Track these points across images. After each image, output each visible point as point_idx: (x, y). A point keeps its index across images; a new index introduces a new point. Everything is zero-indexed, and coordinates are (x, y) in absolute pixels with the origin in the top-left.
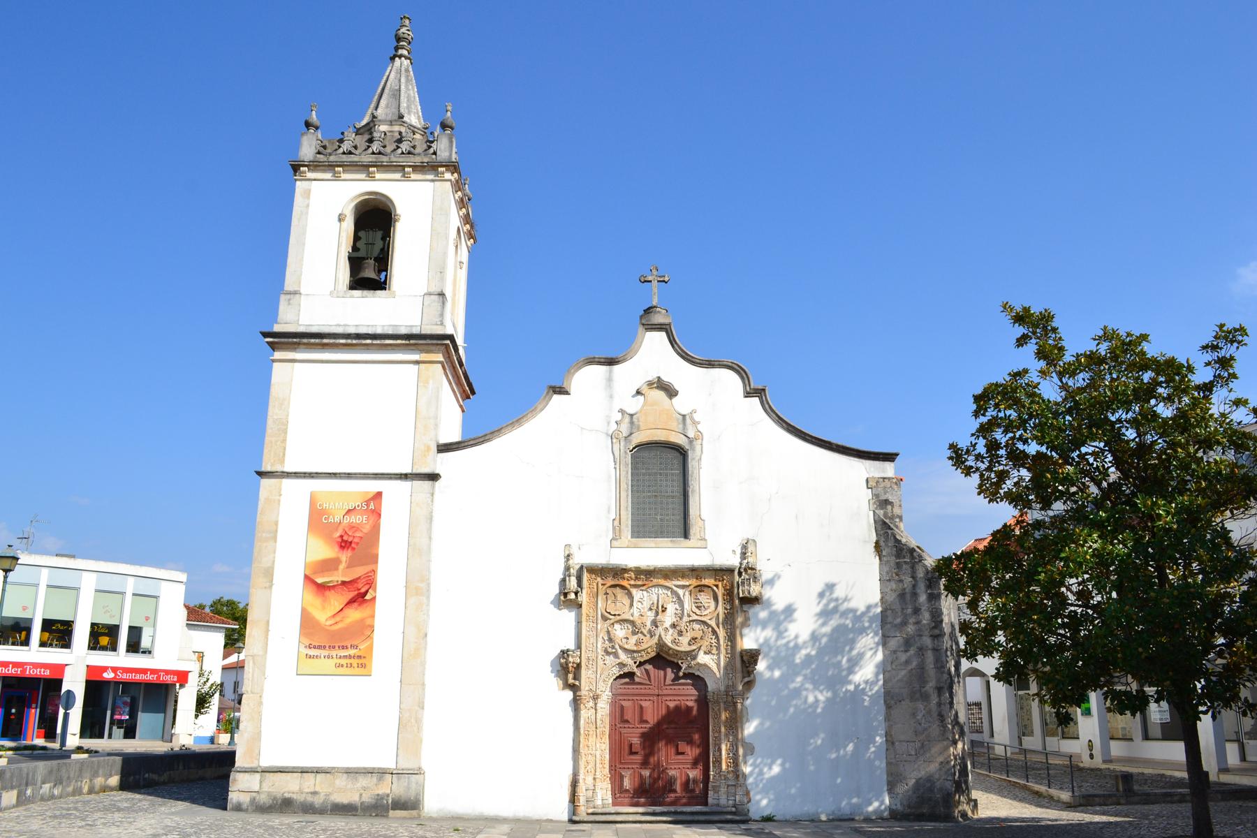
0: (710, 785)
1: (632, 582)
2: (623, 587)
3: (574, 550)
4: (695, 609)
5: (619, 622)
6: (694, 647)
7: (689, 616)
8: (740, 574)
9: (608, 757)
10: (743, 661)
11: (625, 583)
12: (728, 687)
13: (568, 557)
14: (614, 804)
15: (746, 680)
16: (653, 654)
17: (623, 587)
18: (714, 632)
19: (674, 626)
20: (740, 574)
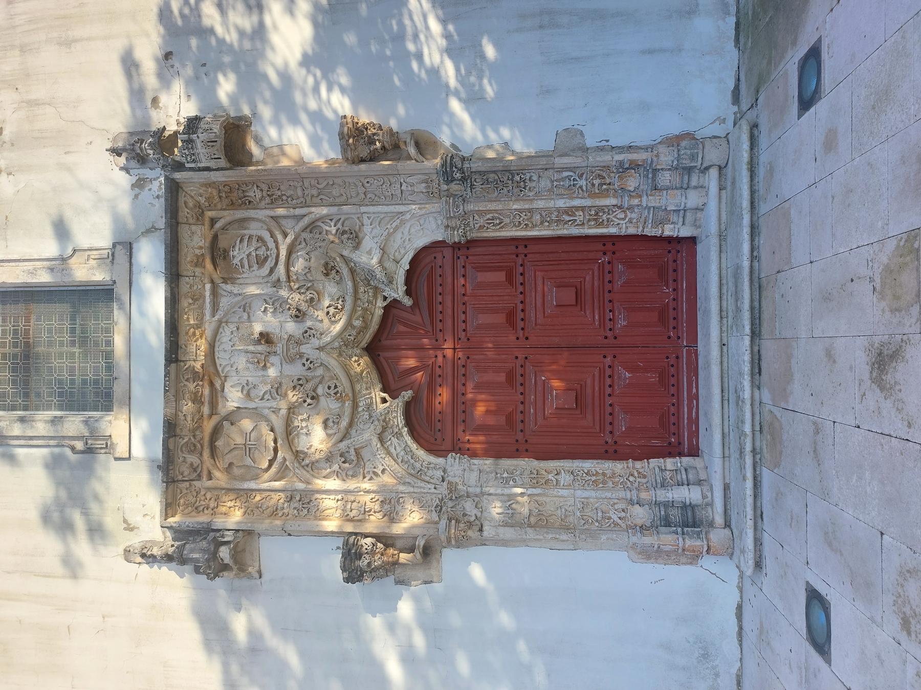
0: (650, 231)
1: (206, 410)
2: (216, 432)
3: (135, 541)
4: (265, 270)
5: (290, 444)
6: (345, 271)
7: (277, 284)
8: (179, 166)
9: (588, 465)
10: (373, 158)
11: (208, 426)
12: (429, 194)
13: (148, 558)
14: (694, 452)
15: (412, 150)
16: (365, 361)
17: (216, 432)
18: (312, 227)
19: (299, 316)
20: (179, 166)
